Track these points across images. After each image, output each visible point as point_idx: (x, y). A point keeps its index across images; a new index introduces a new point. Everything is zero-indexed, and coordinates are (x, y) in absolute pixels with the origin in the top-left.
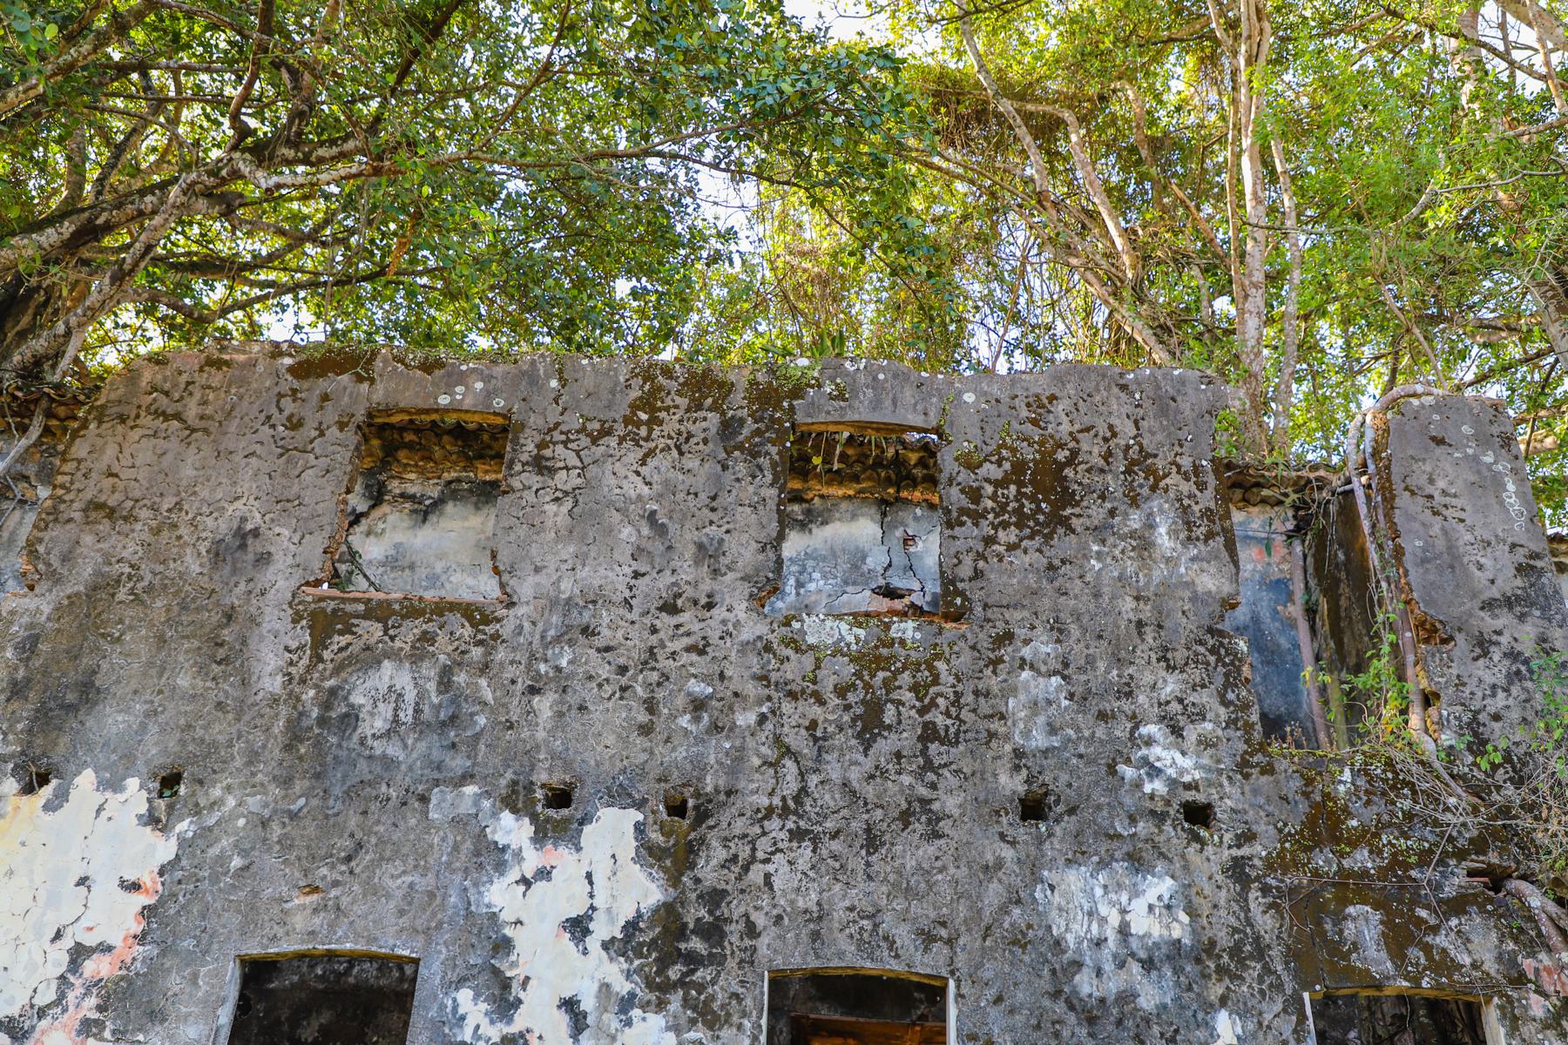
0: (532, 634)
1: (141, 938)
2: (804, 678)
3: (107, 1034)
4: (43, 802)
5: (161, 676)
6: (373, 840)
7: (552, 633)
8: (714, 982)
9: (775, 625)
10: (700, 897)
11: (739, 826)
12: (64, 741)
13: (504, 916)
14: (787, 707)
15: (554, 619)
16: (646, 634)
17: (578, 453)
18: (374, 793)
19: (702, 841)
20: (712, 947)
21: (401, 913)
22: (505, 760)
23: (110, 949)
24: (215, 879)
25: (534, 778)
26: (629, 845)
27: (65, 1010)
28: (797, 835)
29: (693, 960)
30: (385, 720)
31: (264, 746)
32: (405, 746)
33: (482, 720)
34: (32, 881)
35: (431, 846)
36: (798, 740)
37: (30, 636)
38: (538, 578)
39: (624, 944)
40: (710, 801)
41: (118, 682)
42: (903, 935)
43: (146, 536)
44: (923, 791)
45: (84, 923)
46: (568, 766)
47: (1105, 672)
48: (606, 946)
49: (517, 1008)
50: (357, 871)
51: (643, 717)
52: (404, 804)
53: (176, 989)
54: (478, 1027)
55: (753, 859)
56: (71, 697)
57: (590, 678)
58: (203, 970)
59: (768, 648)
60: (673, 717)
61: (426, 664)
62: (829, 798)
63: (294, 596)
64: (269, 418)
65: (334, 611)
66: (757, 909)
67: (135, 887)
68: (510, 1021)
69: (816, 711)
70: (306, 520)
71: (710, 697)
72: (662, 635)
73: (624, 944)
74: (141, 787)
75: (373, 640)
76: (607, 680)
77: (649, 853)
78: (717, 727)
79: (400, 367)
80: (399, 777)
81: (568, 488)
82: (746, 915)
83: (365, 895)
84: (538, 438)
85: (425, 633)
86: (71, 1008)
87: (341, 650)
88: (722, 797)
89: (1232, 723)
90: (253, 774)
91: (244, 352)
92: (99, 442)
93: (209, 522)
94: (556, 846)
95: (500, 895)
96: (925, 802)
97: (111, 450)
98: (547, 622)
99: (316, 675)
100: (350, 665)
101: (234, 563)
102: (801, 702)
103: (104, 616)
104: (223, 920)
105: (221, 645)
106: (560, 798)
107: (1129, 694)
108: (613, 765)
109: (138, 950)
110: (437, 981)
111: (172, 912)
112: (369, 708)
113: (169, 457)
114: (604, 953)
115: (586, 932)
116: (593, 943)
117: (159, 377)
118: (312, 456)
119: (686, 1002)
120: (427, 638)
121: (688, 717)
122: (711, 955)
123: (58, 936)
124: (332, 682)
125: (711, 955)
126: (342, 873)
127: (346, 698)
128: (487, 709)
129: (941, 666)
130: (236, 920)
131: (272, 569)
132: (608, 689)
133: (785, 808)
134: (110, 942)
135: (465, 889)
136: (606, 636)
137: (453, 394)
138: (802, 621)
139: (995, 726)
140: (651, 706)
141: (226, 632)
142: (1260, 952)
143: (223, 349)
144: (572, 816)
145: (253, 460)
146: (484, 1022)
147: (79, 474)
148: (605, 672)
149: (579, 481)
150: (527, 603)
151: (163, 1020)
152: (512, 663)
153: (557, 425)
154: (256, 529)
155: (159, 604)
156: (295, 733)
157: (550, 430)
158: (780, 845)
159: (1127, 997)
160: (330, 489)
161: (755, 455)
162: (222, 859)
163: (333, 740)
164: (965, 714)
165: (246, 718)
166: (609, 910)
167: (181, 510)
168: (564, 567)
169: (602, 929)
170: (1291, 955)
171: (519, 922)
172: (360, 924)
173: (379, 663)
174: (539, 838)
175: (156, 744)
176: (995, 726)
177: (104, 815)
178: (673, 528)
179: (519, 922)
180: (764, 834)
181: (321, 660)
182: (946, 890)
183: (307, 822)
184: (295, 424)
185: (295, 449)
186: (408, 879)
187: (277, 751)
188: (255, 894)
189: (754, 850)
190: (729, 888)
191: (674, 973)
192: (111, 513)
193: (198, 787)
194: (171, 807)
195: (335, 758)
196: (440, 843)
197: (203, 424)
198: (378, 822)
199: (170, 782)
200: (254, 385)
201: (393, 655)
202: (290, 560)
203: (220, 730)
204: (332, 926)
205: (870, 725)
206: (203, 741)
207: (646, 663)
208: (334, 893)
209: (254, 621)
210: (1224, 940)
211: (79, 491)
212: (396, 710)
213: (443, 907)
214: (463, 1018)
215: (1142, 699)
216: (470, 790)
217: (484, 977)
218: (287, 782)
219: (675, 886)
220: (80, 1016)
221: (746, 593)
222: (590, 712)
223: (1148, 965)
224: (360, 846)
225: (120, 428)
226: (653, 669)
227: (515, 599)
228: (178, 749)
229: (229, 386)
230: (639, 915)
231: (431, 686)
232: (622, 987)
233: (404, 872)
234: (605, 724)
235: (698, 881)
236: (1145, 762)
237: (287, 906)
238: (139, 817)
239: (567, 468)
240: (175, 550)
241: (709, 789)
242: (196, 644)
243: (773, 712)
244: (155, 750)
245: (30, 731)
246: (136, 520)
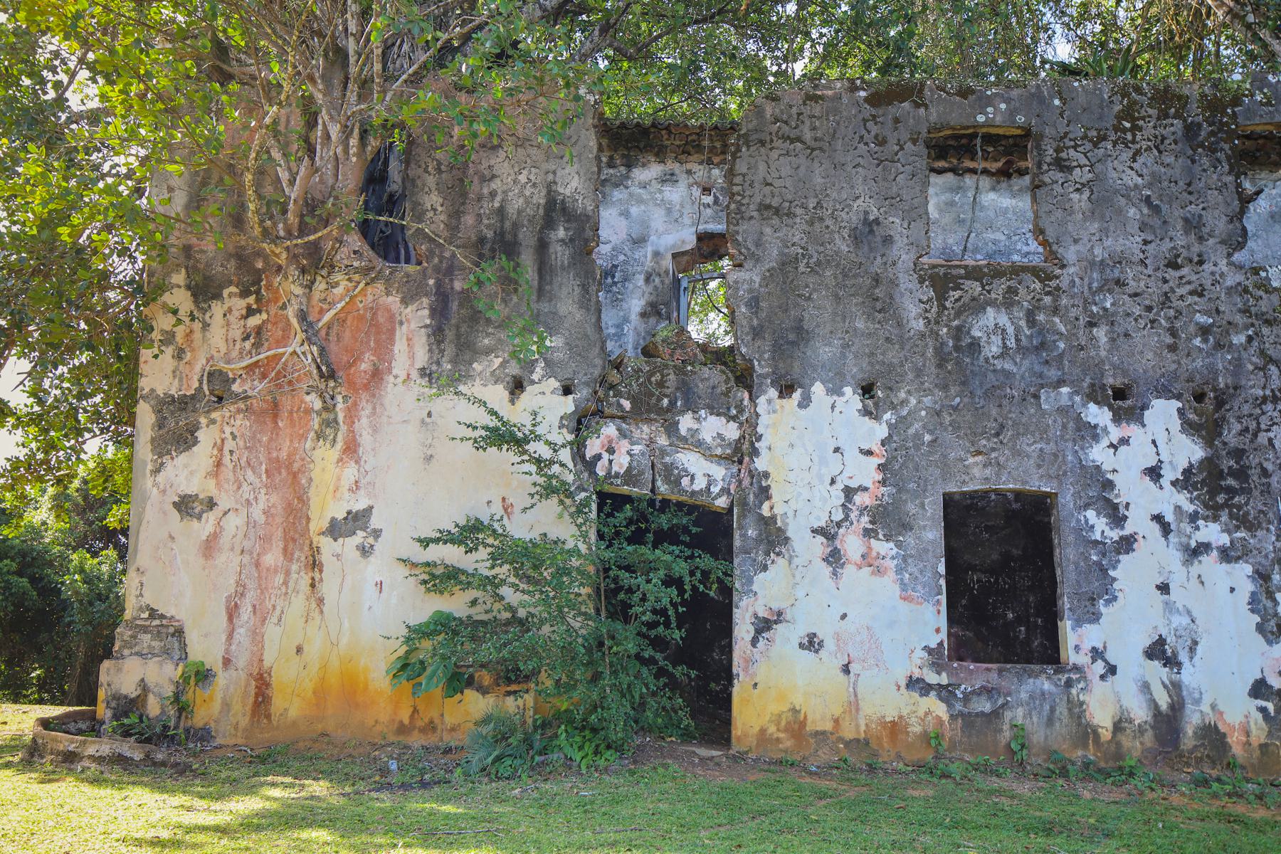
0: (1082, 286)
1: (883, 483)
2: (1274, 311)
3: (881, 536)
4: (796, 403)
5: (844, 322)
6: (1010, 423)
7: (1095, 285)
8: (1247, 504)
9: (1249, 275)
10: (1227, 454)
11: (1246, 409)
12: (796, 364)
13: (1104, 467)
14: (1265, 330)
15: (1095, 275)
16: (1160, 284)
17: (1085, 154)
18: (1003, 394)
19: (1224, 419)
20: (1241, 483)
21: (1039, 466)
22: (1083, 370)
23: (866, 489)
24: (917, 448)
25: (1105, 382)
26: (1176, 424)
27: (852, 523)
29: (1231, 491)
30: (998, 346)
31: (924, 365)
32: (1016, 364)
33: (1062, 345)
34: (806, 450)
35: (1048, 425)
37: (753, 298)
38: (1078, 247)
39: (1186, 481)
40: (1224, 394)
41: (818, 326)
43: (805, 227)
45: (846, 474)
46: (1125, 373)
48: (1174, 483)
49: (1125, 521)
50: (1005, 441)
52: (1024, 400)
53: (914, 511)
54: (1103, 532)
55: (1259, 430)
56: (792, 337)
57: (1128, 315)
58: (927, 501)
59: (1246, 291)
60: (1189, 339)
61: (1015, 309)
63: (915, 265)
64: (862, 137)
65: (945, 274)
66: (1266, 460)
67: (869, 453)
68: (1123, 528)
70: (908, 211)
71: (1212, 325)
72: (1171, 284)
73: (1186, 481)
74: (854, 393)
75: (976, 294)
76: (1140, 316)
77: (1189, 427)
78: (1220, 345)
79: (944, 95)
80: (1017, 383)
81: (1084, 180)
82: (1261, 464)
83: (1013, 456)
84: (1055, 145)
85: (1009, 287)
86: (855, 522)
87: (957, 300)
88: (1232, 391)
90: (922, 383)
91: (831, 89)
92: (752, 161)
93: (843, 214)
94: (1128, 424)
95: (1098, 454)
97: (762, 167)
98: (1091, 278)
99: (945, 318)
100: (965, 311)
101: (869, 244)
102: (1274, 328)
103: (795, 282)
104: (930, 473)
105: (877, 299)
106: (1120, 394)
108: (1156, 372)
109: (883, 489)
110: (1072, 506)
111: (896, 467)
112: (985, 339)
113: (802, 169)
114: (1173, 488)
115: (1160, 476)
116: (1165, 482)
117: (777, 110)
118: (899, 165)
119: (1231, 516)
120: (1011, 291)
121: (1199, 339)
122: (1241, 488)
123: (833, 482)
124: (956, 323)
125: (1241, 488)
126: (996, 443)
127: (968, 333)
128: (1063, 337)
130: (938, 472)
131: (895, 247)
132: (1142, 322)
133: (1274, 396)
134: (865, 484)
135: (1076, 452)
136: (1133, 286)
137: (986, 114)
138: (1267, 271)
140: (1173, 332)
141: (877, 291)
143: (816, 87)
144: (1135, 405)
145: (860, 169)
146: (1107, 529)
147: (747, 184)
148: (1137, 311)
149: (1090, 175)
150: (1074, 265)
151: (911, 529)
152: (1073, 306)
153: (1066, 134)
154: (877, 219)
155: (828, 273)
157: (1062, 138)
158: (1275, 420)
160: (918, 188)
161: (1214, 151)
162: (918, 436)
163: (968, 360)
165: (908, 347)
166: (1171, 462)
167: (822, 207)
168: (1094, 238)
169: (1169, 475)
171: (1115, 471)
172: (1015, 473)
173: (985, 309)
174: (1117, 419)
175: (855, 365)
177: (837, 410)
178: (1165, 208)
179: (1115, 471)
180: (1263, 413)
181: (946, 308)
183: (965, 412)
184: (881, 142)
185: (886, 160)
186: (1039, 446)
187: (933, 368)
188: (945, 456)
189: (1259, 424)
190: (1246, 447)
191: (1221, 499)
192: (777, 211)
193: (889, 392)
194: (876, 405)
195: (972, 371)
196: (1054, 424)
197: (817, 144)
198: (1010, 412)
199: (867, 390)
200: (845, 113)
201: (992, 303)
202: (905, 241)
203: (893, 355)
204: (998, 475)
206: (884, 363)
207: (1164, 303)
208: (993, 455)
209: (894, 283)
211: (751, 197)
212: (1003, 339)
213: (1064, 462)
214: (1093, 527)
216: (1065, 390)
217: (1101, 503)
218: (945, 388)
219: (1210, 447)
220: (862, 526)
221: (1225, 252)
222: (1132, 338)
224: (1002, 426)
225: (762, 150)
226: (1170, 307)
227: (1065, 262)
228: (869, 368)
229: (828, 115)
230: (1191, 465)
231: (1023, 323)
232: (1190, 508)
233: (1035, 442)
234: (1144, 345)
235: (1225, 444)
237: (966, 463)
238: (859, 411)
239: (1079, 166)
240: (827, 236)
241: (1222, 386)
242: (861, 300)
243: (1256, 334)
244: (855, 368)
245: (773, 358)
246: (795, 216)
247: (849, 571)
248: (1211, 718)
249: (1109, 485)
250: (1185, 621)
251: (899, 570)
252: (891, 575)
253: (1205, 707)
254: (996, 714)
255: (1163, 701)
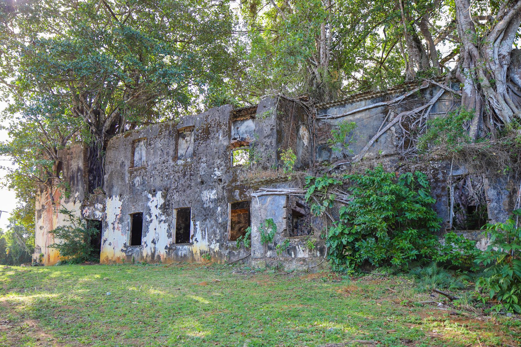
1: (121, 213)
11: (171, 191)
14: (176, 174)
19: (167, 194)
28: (177, 192)
29: (167, 209)
36: (177, 179)
42: (187, 202)
44: (190, 183)
47: (212, 161)
51: (161, 179)
62: (180, 186)
67: (119, 208)
69: (179, 174)
73: (160, 208)
77: (163, 196)
89: (225, 166)
95: (149, 204)
96: (190, 184)
107: (214, 164)
116: (158, 208)
120: (140, 173)
129: (193, 164)
136: (158, 168)
139: (198, 172)
142: (224, 198)
148: (158, 173)
156: (130, 187)
159: (209, 206)
161: (172, 136)
164: (195, 171)
169: (159, 206)
170: (228, 198)
176: (198, 172)
178: (164, 150)
182: (192, 196)
201: (137, 176)
205: (184, 175)
209: (125, 174)
210: (221, 197)
215: (215, 164)
216: (146, 192)
218: (130, 194)
223: (212, 202)
232: (161, 213)
236: (215, 174)
244: (119, 192)
247: (116, 230)
248: (159, 254)
249: (150, 210)
250: (157, 235)
251: (122, 229)
252: (121, 231)
253: (158, 252)
254: (131, 255)
255: (153, 251)
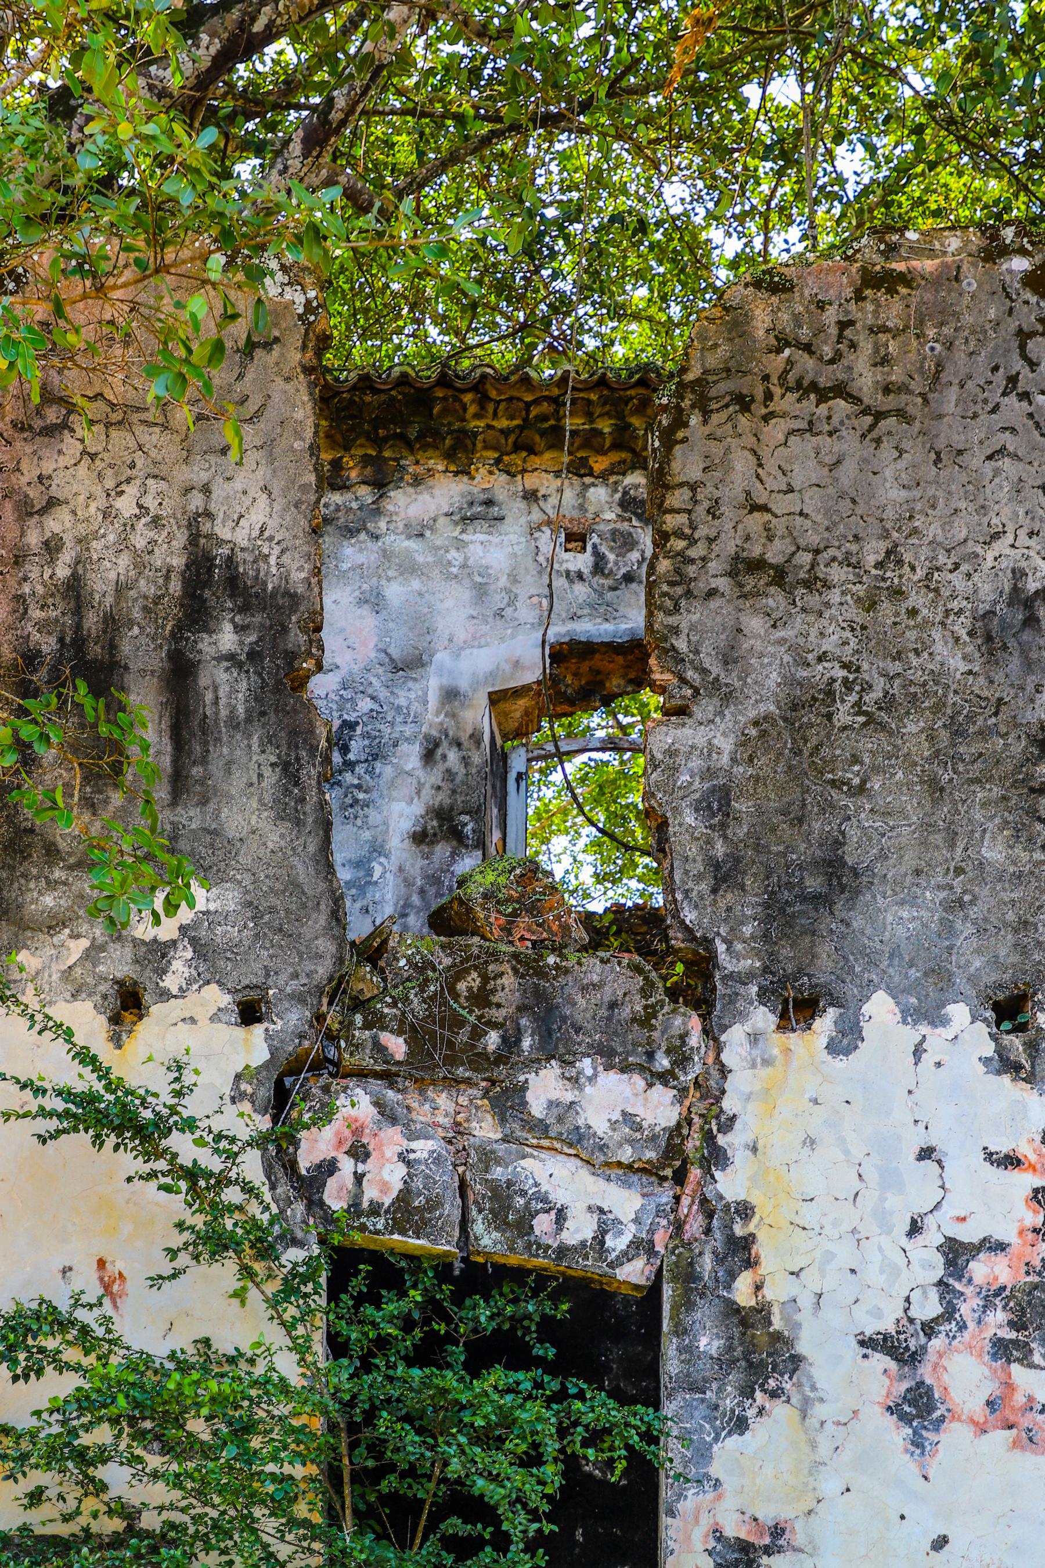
64: (1013, 380)
91: (932, 254)
92: (716, 449)
93: (957, 580)
97: (742, 464)
113: (848, 471)
117: (785, 317)
145: (1006, 463)
147: (701, 510)
167: (900, 563)
192: (779, 576)
197: (891, 402)
200: (968, 319)
211: (711, 540)
225: (743, 421)
229: (921, 323)
240: (911, 635)
246: (827, 585)
